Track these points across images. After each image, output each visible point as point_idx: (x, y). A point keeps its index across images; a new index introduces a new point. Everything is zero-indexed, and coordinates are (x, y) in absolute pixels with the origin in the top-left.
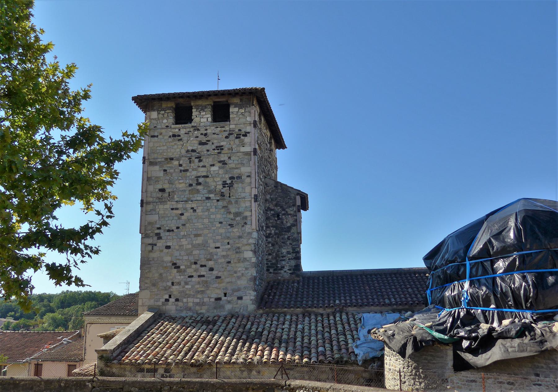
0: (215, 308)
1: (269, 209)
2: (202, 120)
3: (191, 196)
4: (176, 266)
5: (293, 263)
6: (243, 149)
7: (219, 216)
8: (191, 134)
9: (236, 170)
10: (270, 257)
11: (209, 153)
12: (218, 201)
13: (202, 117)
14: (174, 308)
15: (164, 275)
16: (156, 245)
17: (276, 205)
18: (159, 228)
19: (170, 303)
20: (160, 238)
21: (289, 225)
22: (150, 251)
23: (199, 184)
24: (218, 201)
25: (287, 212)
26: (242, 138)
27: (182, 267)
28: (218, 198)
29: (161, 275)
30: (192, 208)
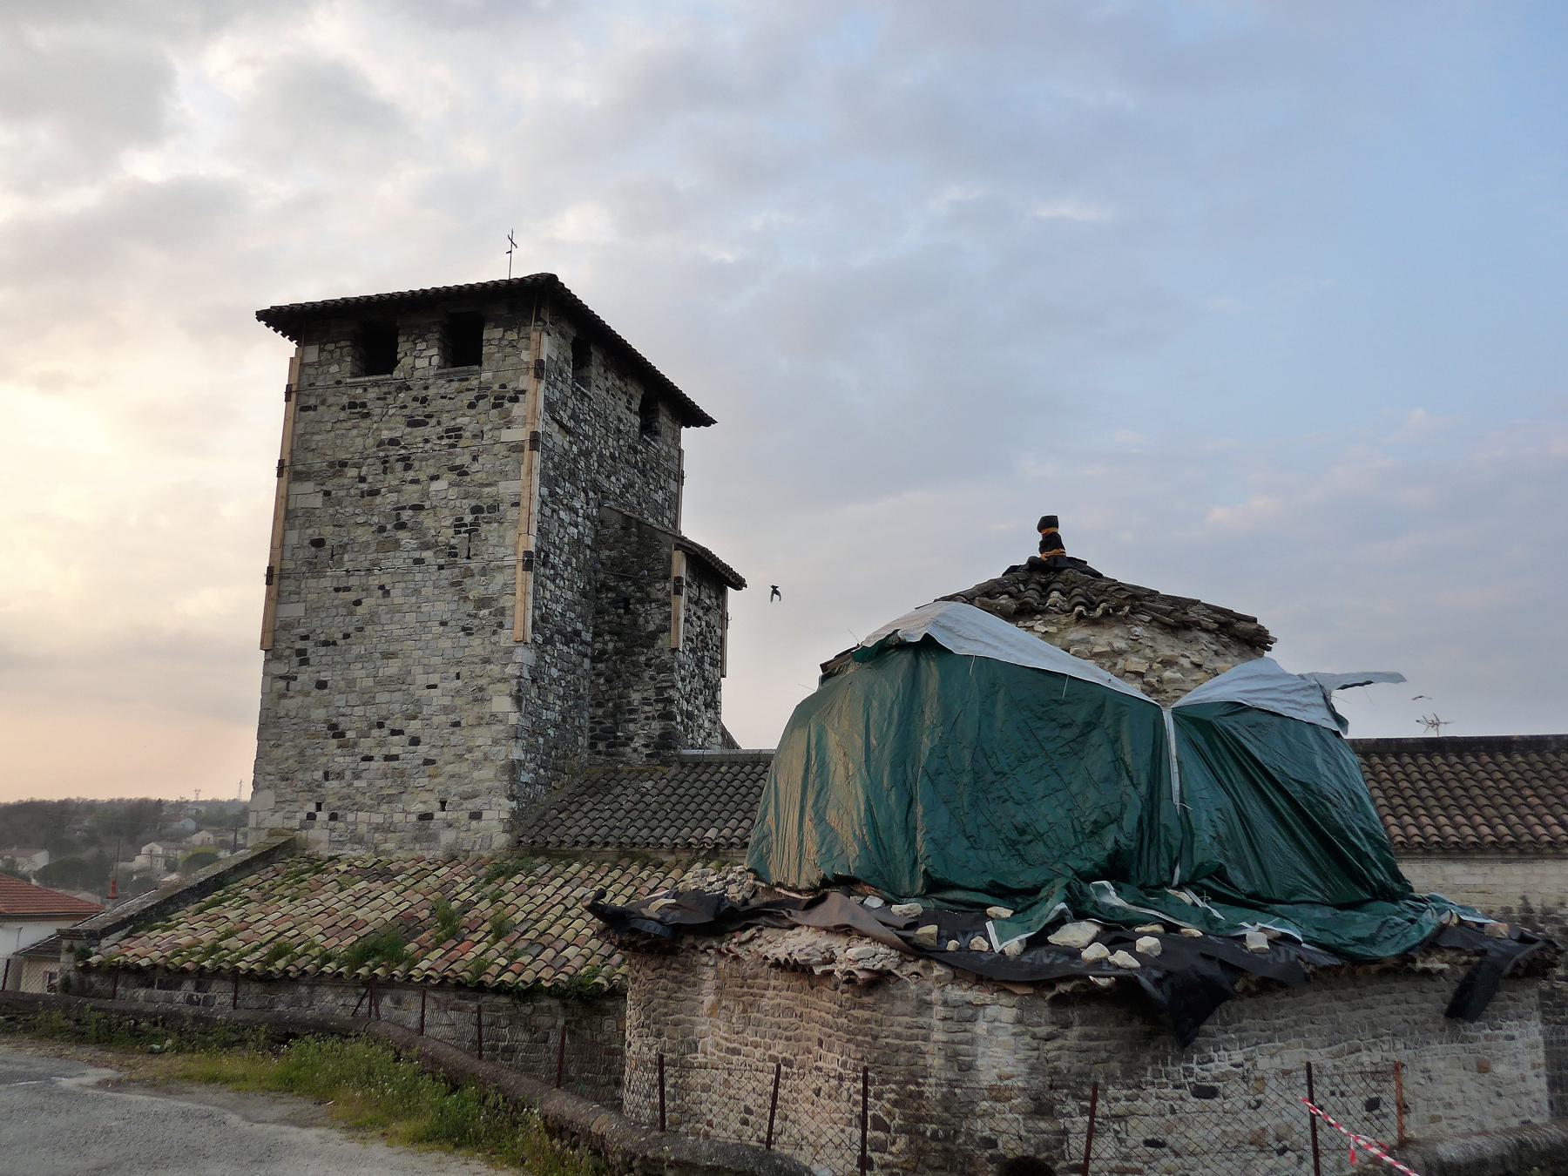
0: (416, 839)
1: (604, 587)
2: (420, 363)
3: (381, 556)
4: (336, 732)
5: (656, 727)
6: (509, 435)
7: (440, 606)
8: (390, 399)
9: (487, 490)
10: (600, 712)
11: (428, 446)
12: (441, 567)
13: (421, 359)
14: (324, 835)
15: (309, 752)
16: (295, 679)
17: (623, 579)
18: (305, 638)
19: (317, 825)
20: (305, 662)
21: (652, 627)
22: (282, 696)
23: (401, 526)
24: (441, 567)
25: (648, 594)
26: (507, 405)
27: (350, 735)
28: (442, 561)
29: (301, 753)
30: (382, 587)
